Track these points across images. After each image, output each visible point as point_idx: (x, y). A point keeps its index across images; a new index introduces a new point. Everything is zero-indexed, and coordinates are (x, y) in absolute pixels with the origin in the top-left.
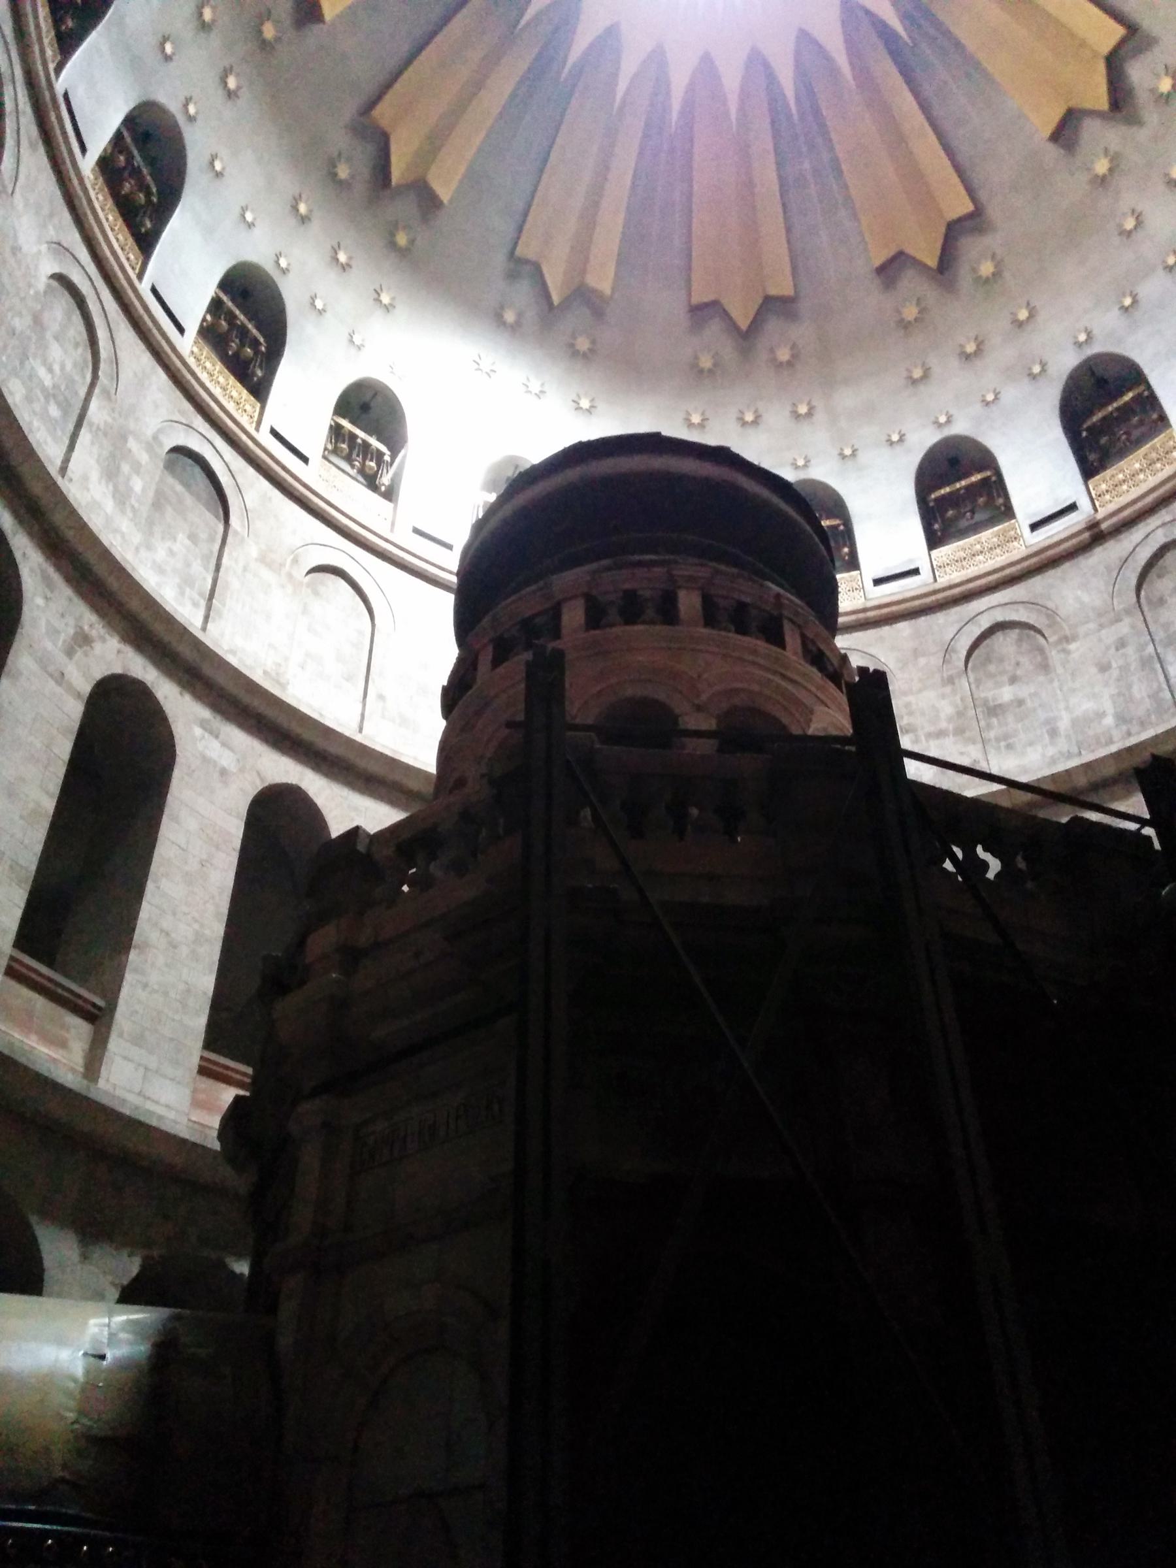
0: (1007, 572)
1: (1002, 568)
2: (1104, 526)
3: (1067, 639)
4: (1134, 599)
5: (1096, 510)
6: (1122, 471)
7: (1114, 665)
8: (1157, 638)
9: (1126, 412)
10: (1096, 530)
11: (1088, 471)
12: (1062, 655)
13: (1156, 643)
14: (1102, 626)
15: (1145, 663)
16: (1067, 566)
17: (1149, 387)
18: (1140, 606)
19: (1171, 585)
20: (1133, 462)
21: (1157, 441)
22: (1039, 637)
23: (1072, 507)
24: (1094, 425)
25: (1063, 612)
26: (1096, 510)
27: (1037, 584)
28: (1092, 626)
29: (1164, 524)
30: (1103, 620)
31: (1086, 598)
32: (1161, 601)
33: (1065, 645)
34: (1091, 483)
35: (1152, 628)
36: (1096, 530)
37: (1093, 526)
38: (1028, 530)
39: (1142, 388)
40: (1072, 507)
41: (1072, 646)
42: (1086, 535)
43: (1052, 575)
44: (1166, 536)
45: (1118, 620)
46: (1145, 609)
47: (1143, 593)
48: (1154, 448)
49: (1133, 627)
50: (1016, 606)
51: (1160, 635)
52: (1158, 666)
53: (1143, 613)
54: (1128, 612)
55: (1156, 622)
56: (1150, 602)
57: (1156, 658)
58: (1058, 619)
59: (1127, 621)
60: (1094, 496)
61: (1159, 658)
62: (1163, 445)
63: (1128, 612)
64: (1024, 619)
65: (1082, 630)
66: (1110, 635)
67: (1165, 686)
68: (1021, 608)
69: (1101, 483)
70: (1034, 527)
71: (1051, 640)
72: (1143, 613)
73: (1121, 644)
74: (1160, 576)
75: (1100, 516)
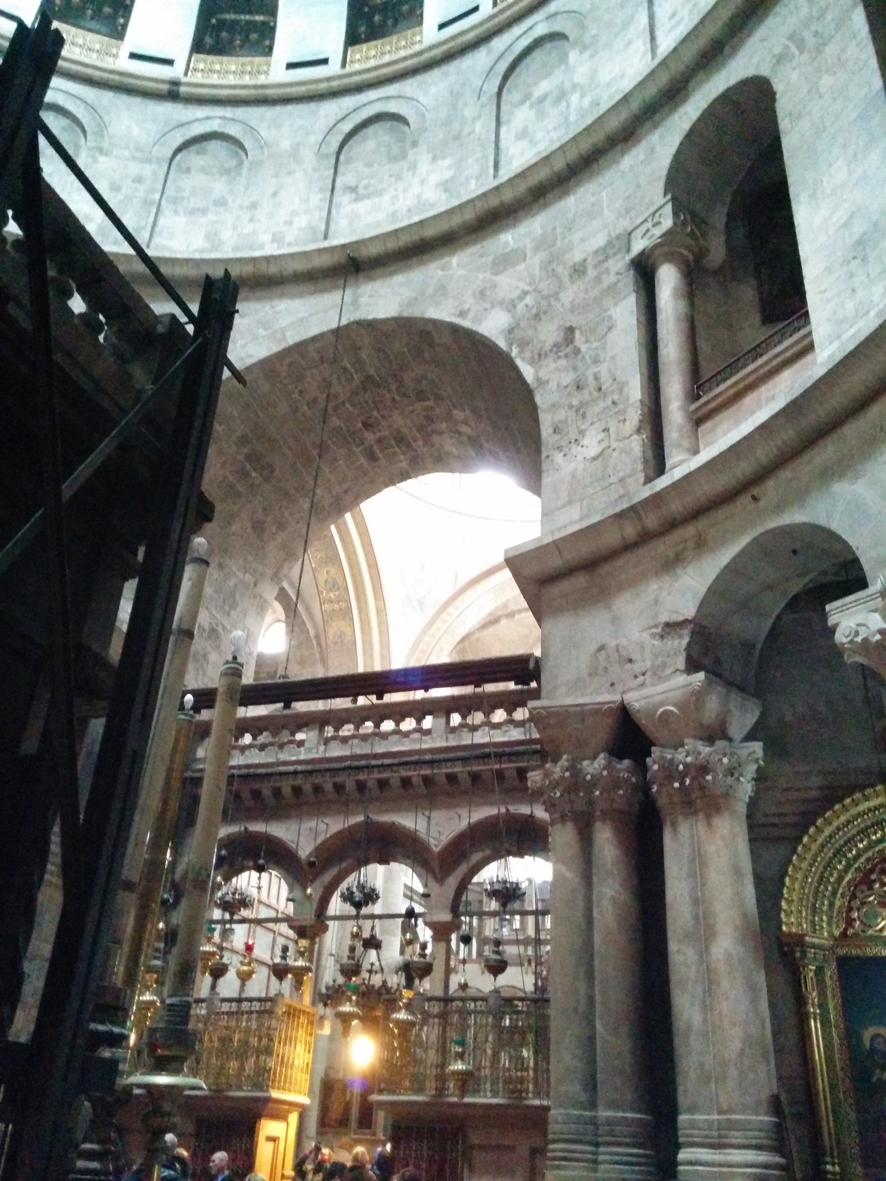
0: (89, 71)
1: (86, 65)
2: (183, 89)
3: (101, 151)
4: (170, 155)
5: (186, 74)
6: (221, 63)
7: (124, 190)
8: (167, 192)
9: (252, 26)
10: (175, 88)
11: (198, 47)
12: (90, 160)
13: (164, 196)
14: (133, 158)
15: (147, 203)
16: (137, 101)
17: (275, 22)
18: (170, 164)
19: (201, 163)
20: (231, 63)
21: (257, 60)
22: (82, 136)
23: (169, 62)
24: (225, 20)
25: (112, 130)
26: (186, 74)
27: (106, 97)
28: (126, 153)
29: (223, 118)
30: (138, 155)
31: (135, 131)
32: (188, 170)
33: (97, 154)
34: (195, 56)
35: (168, 184)
36: (175, 88)
37: (175, 83)
38: (128, 55)
39: (272, 19)
40: (169, 62)
41: (102, 159)
42: (165, 87)
43: (122, 101)
44: (220, 126)
45: (148, 161)
46: (173, 167)
47: (178, 157)
48: (252, 64)
49: (155, 173)
50: (78, 102)
51: (170, 191)
52: (154, 210)
53: (169, 168)
54: (159, 161)
55: (174, 181)
56: (179, 165)
57: (156, 205)
58: (106, 133)
59: (155, 166)
60: (191, 67)
61: (159, 205)
62: (259, 65)
63: (159, 161)
64: (79, 116)
65: (116, 152)
66: (134, 169)
67: (149, 228)
68: (82, 106)
69: (202, 61)
70: (133, 56)
71: (89, 143)
72: (169, 168)
73: (139, 180)
74: (198, 153)
75: (184, 80)
